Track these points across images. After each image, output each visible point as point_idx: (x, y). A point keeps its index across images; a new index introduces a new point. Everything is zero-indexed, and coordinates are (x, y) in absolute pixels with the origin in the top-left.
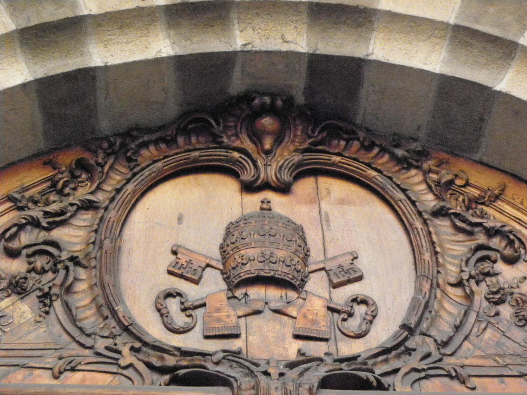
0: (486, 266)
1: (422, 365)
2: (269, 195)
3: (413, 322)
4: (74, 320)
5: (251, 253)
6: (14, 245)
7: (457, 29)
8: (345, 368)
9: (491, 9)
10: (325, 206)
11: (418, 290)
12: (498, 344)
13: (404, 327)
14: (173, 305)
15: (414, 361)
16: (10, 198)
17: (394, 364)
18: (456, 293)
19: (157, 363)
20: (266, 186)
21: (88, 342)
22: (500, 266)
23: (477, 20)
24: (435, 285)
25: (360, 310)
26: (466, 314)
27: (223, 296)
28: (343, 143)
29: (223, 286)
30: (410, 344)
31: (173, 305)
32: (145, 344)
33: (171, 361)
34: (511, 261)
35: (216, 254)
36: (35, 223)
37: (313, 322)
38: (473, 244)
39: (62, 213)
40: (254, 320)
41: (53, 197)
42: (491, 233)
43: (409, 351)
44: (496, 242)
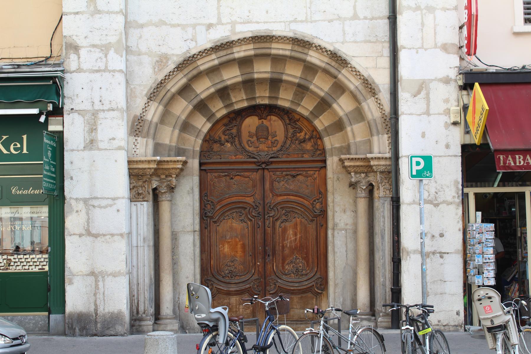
0: (295, 134)
1: (283, 153)
2: (263, 120)
3: (283, 145)
4: (236, 147)
5: (260, 134)
6: (226, 134)
7: (291, 101)
8: (273, 155)
9: (297, 97)
10: (272, 122)
11: (284, 139)
12: (295, 148)
13: (282, 146)
14: (249, 142)
15: (282, 152)
16: (224, 125)
17: (280, 152)
18: (289, 139)
19: (248, 154)
20: (263, 119)
21: (238, 150)
22: (297, 134)
23: (295, 99)
24: (287, 138)
25: (276, 142)
26: (291, 143)
27: (256, 141)
28: (275, 110)
29: (256, 139)
30: (282, 149)
31: (249, 142)
32: (246, 151)
33: (250, 154)
34: (299, 133)
35: (255, 133)
36: (228, 130)
37: (269, 145)
38: (294, 130)
39: (232, 127)
40: (260, 144)
41: (230, 124)
42: (296, 128)
43: (282, 150)
44: (297, 130)
